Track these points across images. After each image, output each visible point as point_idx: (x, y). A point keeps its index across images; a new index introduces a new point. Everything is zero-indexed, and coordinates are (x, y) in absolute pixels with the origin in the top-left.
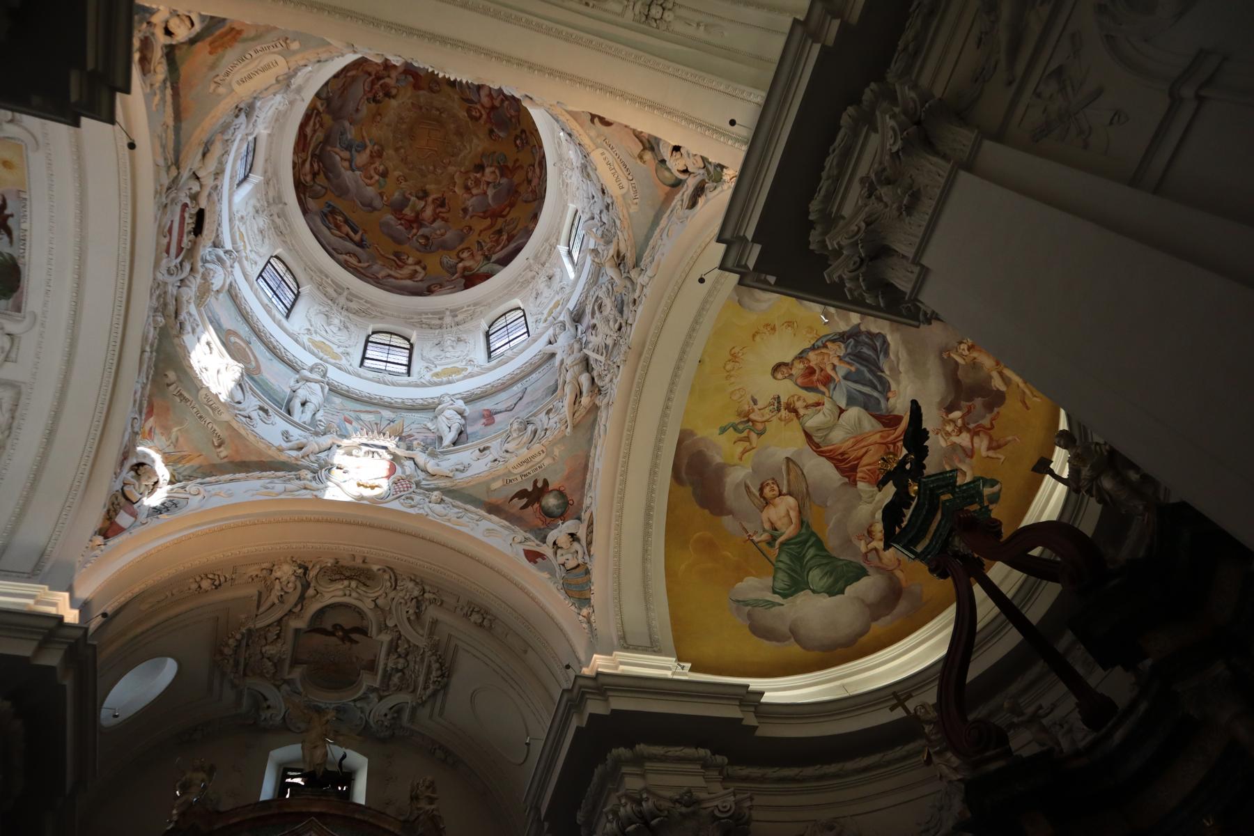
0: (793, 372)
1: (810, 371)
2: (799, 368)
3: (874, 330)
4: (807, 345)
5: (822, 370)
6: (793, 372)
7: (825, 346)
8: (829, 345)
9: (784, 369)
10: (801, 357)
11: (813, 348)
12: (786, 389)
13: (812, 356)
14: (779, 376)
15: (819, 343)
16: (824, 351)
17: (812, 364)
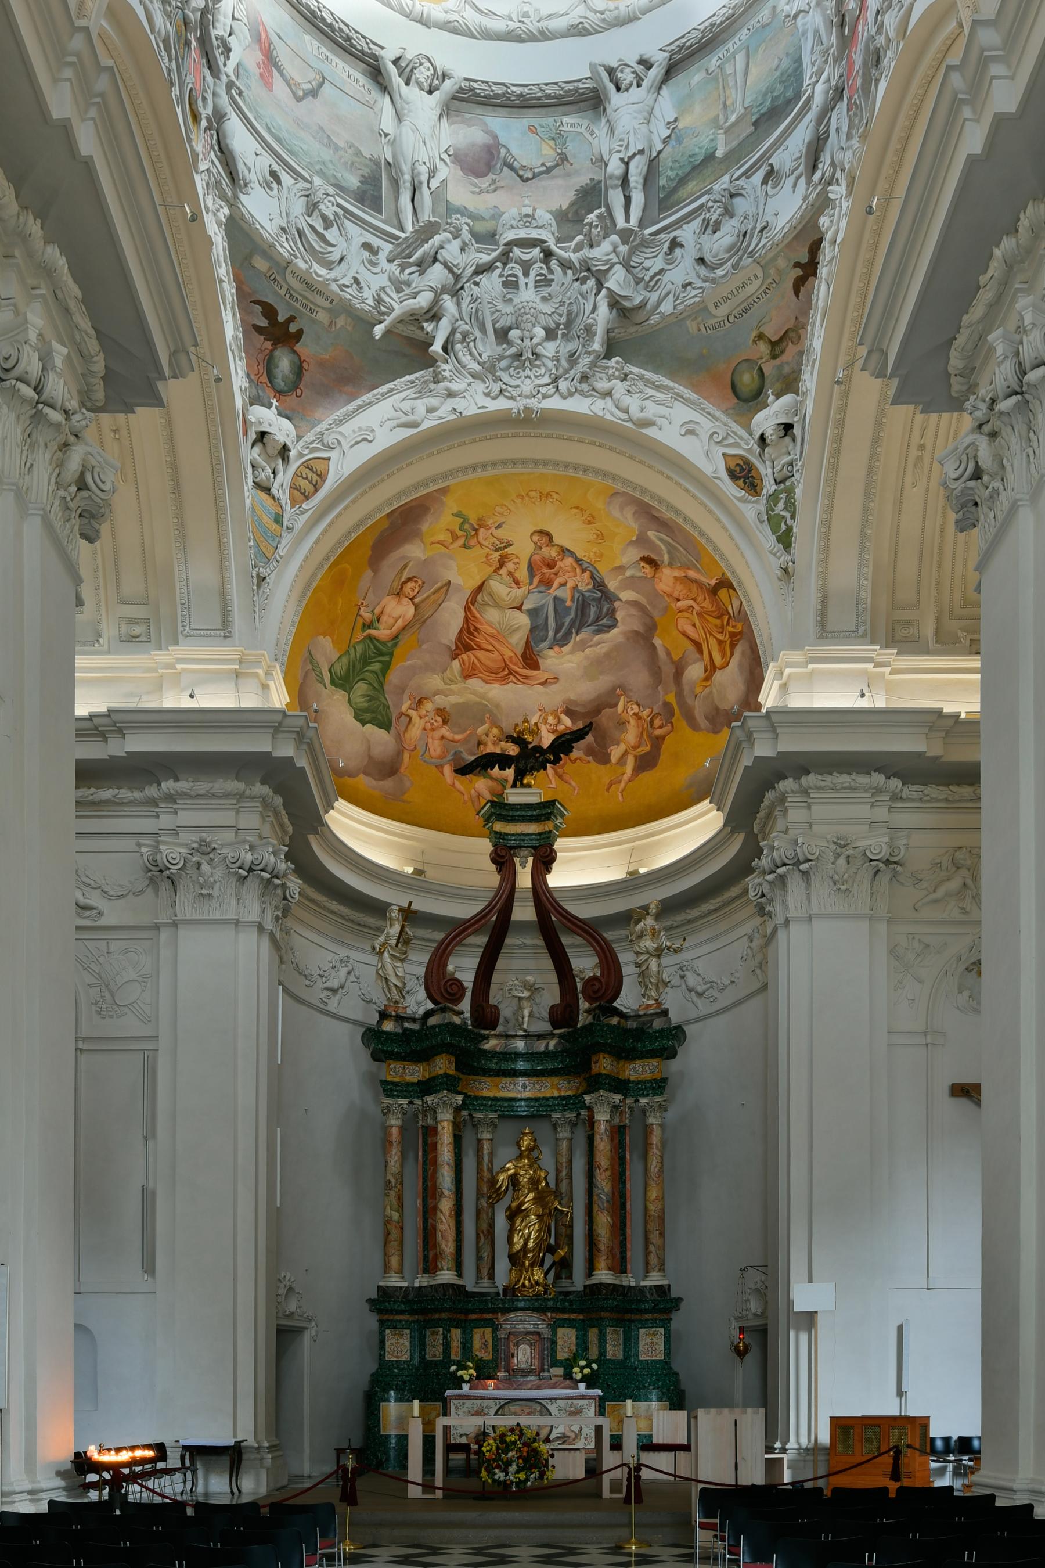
0: (544, 549)
1: (551, 564)
2: (554, 553)
3: (619, 615)
4: (580, 554)
5: (556, 574)
6: (544, 549)
7: (584, 571)
8: (587, 574)
9: (545, 539)
10: (564, 551)
11: (578, 560)
12: (523, 548)
13: (569, 561)
14: (536, 538)
15: (585, 565)
16: (578, 571)
17: (560, 564)
